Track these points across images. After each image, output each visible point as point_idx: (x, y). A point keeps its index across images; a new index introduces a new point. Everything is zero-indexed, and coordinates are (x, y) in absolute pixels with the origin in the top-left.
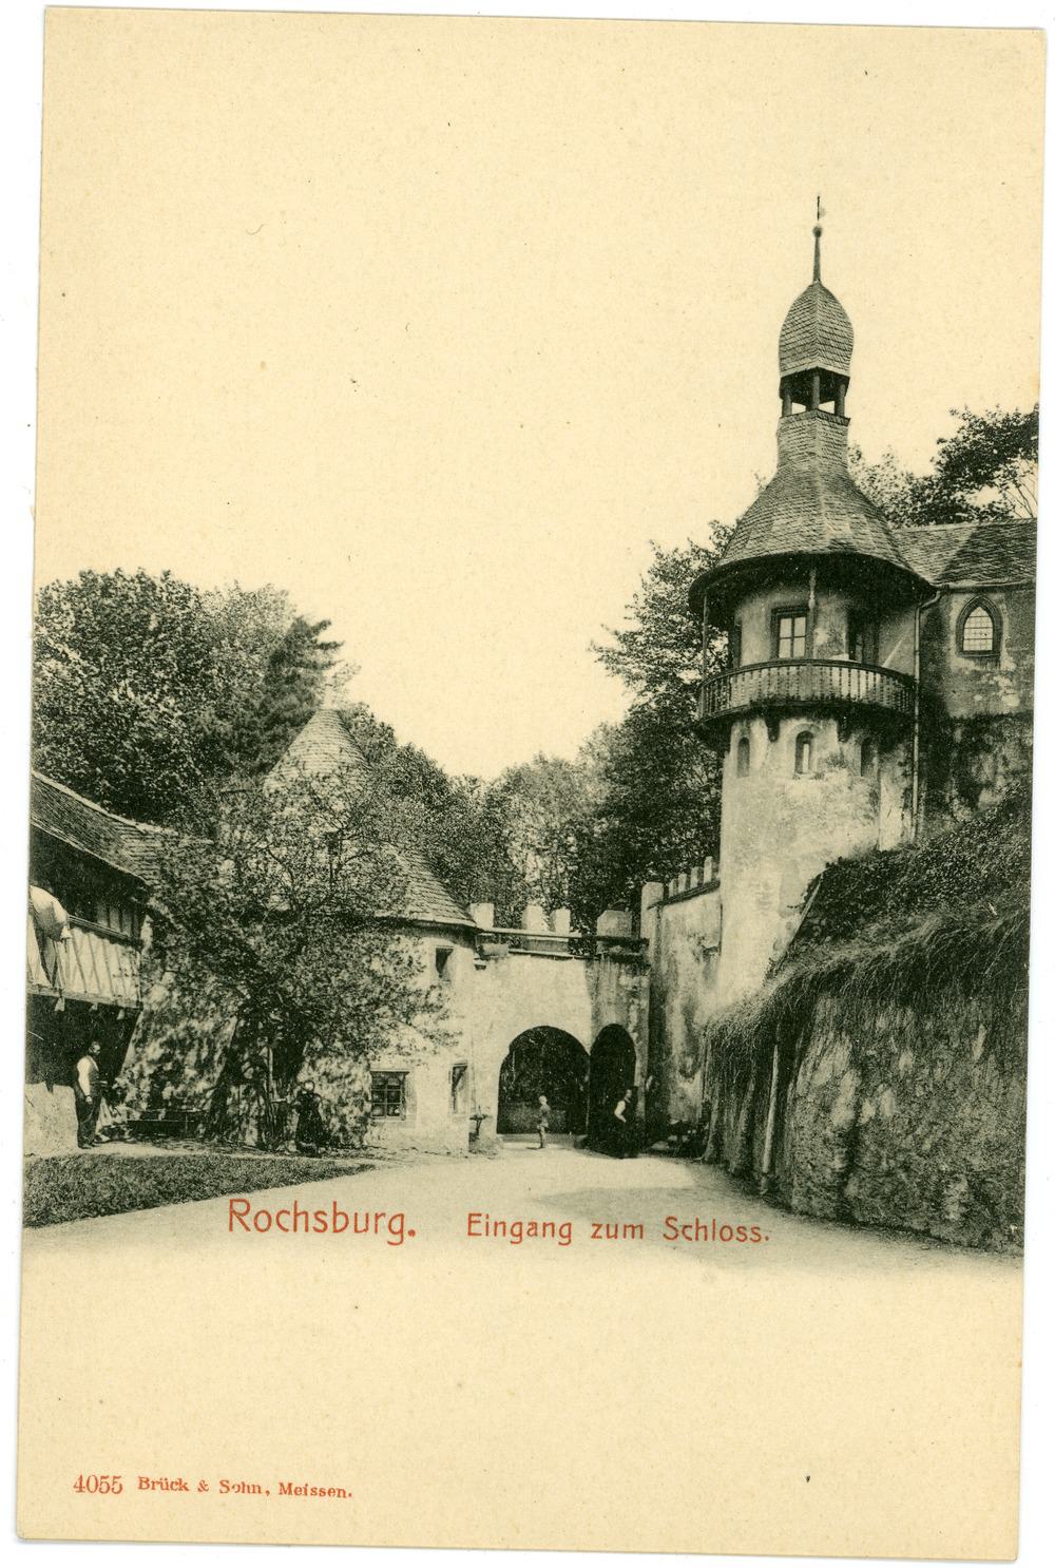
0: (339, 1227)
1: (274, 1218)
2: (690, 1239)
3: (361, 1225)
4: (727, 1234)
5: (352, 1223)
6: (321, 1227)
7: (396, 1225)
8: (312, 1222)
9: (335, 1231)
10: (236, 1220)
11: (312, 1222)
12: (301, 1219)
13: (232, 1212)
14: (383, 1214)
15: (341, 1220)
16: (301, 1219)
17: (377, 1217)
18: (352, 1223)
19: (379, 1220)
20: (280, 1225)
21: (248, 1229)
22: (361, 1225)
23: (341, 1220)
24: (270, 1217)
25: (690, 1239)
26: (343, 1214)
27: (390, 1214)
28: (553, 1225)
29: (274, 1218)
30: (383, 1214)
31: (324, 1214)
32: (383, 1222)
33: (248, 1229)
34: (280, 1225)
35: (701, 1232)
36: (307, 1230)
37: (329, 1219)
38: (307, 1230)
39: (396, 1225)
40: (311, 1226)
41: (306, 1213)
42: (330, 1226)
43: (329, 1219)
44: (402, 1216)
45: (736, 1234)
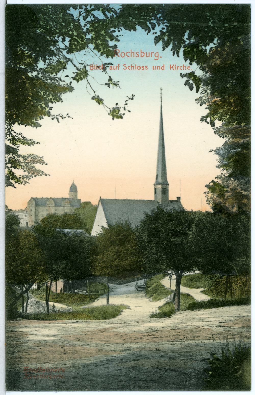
0: (142, 55)
1: (126, 55)
2: (129, 69)
3: (148, 55)
4: (139, 68)
5: (145, 55)
6: (137, 56)
7: (156, 55)
8: (136, 55)
9: (141, 57)
11: (136, 55)
12: (133, 54)
14: (153, 52)
16: (133, 54)
20: (127, 56)
22: (148, 55)
24: (124, 54)
25: (129, 69)
27: (155, 53)
29: (125, 54)
30: (153, 52)
32: (153, 55)
34: (127, 56)
35: (133, 67)
36: (134, 57)
37: (140, 54)
38: (134, 57)
39: (156, 55)
40: (135, 56)
41: (134, 52)
42: (140, 56)
43: (140, 54)
45: (141, 68)
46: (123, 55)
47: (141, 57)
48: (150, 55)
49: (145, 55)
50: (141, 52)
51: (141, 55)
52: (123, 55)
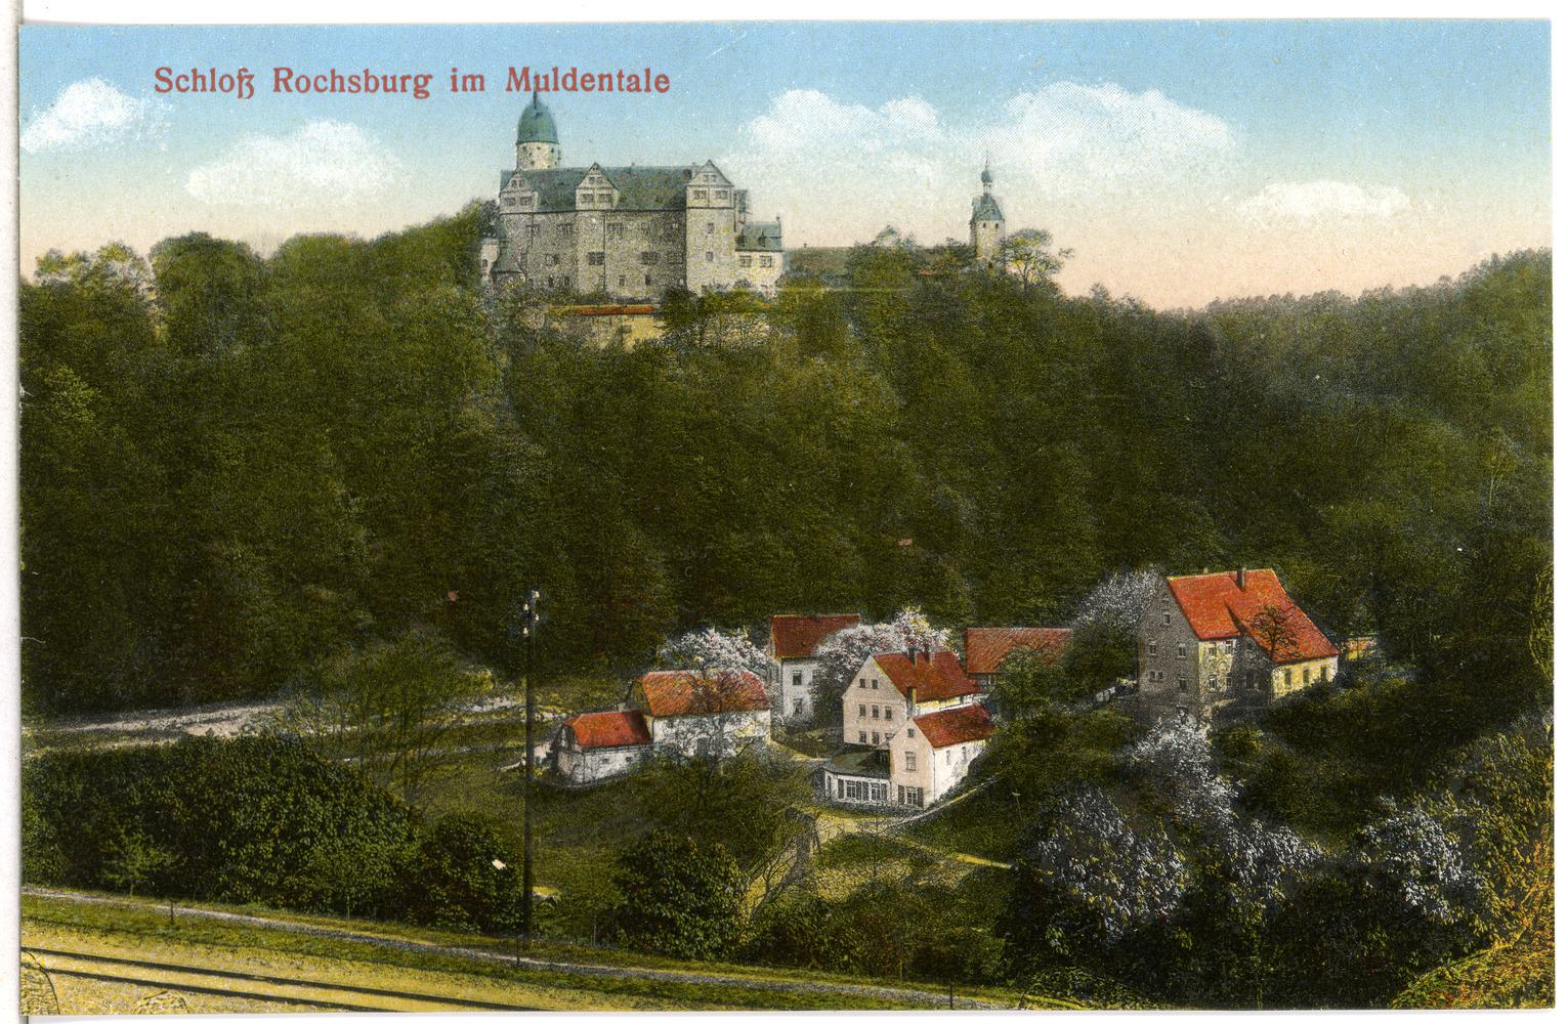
6: (354, 88)
8: (347, 84)
10: (281, 84)
12: (338, 81)
13: (277, 80)
14: (409, 77)
15: (372, 85)
16: (338, 81)
18: (381, 82)
19: (407, 81)
21: (288, 89)
22: (390, 86)
23: (372, 85)
26: (375, 77)
28: (609, 76)
30: (409, 77)
31: (358, 78)
32: (410, 84)
33: (288, 89)
36: (342, 90)
37: (362, 84)
40: (346, 89)
41: (341, 78)
42: (363, 87)
44: (427, 78)
46: (303, 86)
47: (367, 89)
48: (399, 88)
49: (381, 86)
50: (367, 78)
51: (367, 85)
52: (303, 82)
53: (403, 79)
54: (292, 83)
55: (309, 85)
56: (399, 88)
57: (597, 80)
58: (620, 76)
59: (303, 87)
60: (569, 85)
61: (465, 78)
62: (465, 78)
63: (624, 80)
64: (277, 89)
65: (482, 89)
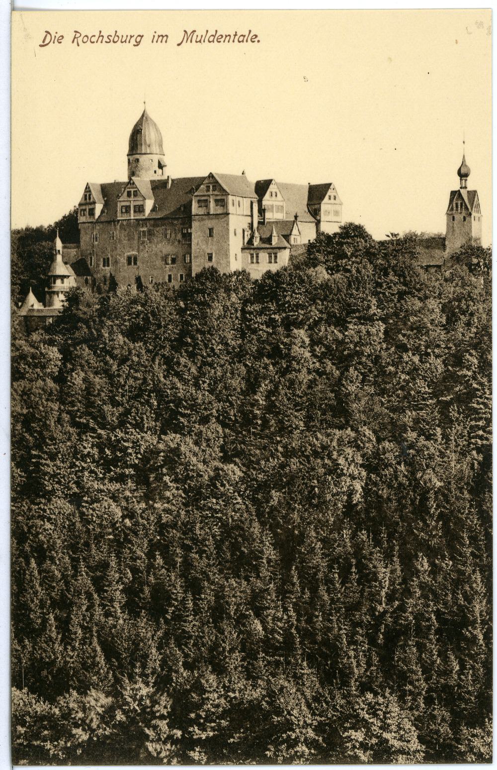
8: (106, 39)
16: (101, 38)
17: (131, 37)
32: (133, 40)
41: (103, 36)
44: (142, 36)
53: (131, 37)
54: (80, 40)
55: (89, 39)
56: (128, 41)
57: (224, 37)
58: (236, 35)
59: (85, 40)
60: (211, 39)
61: (159, 36)
62: (159, 36)
63: (237, 37)
64: (73, 42)
65: (166, 42)
